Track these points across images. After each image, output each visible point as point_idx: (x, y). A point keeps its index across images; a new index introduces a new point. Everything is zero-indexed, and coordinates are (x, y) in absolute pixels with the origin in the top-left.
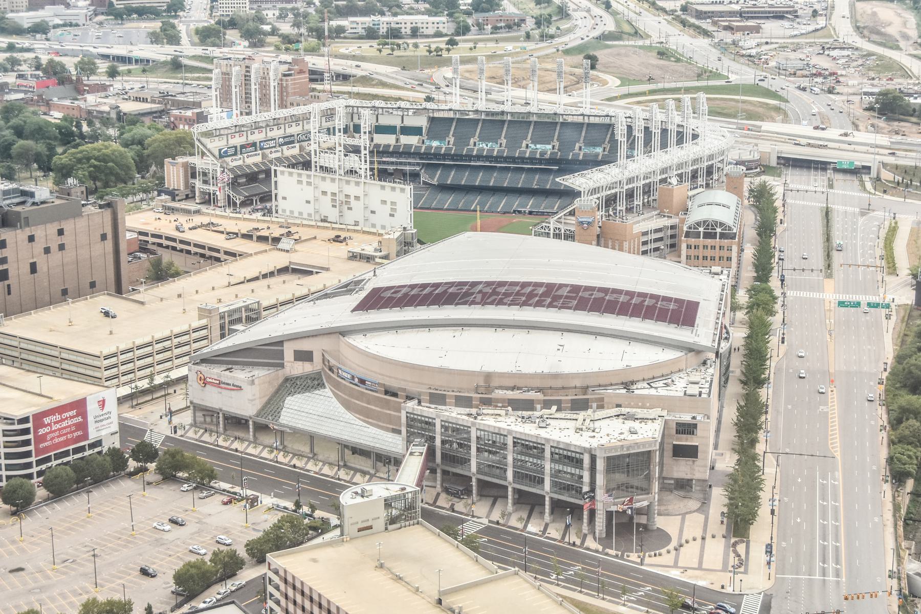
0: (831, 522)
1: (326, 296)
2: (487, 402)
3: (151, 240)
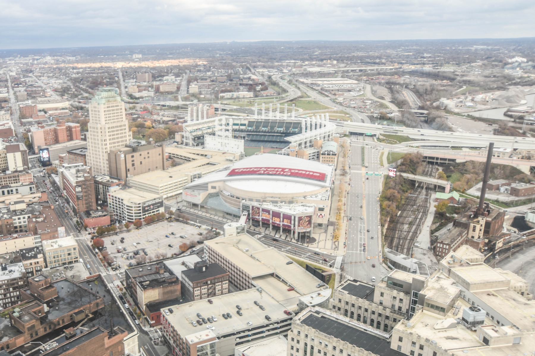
0: (363, 237)
1: (220, 171)
2: (264, 201)
3: (172, 155)
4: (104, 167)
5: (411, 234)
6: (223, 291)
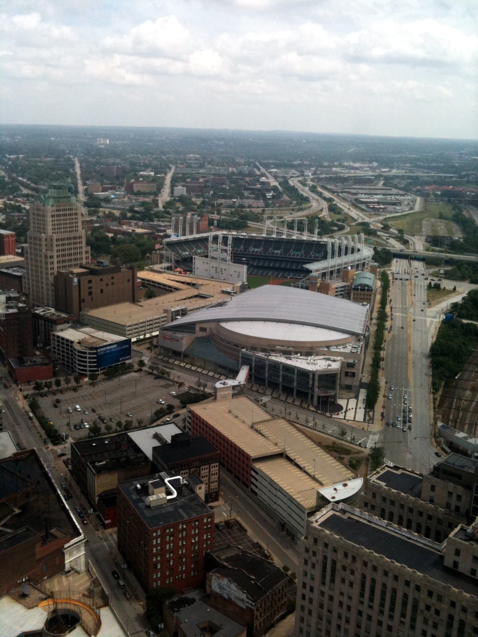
1: (212, 307)
2: (274, 351)
4: (48, 295)
5: (474, 403)
6: (212, 477)
